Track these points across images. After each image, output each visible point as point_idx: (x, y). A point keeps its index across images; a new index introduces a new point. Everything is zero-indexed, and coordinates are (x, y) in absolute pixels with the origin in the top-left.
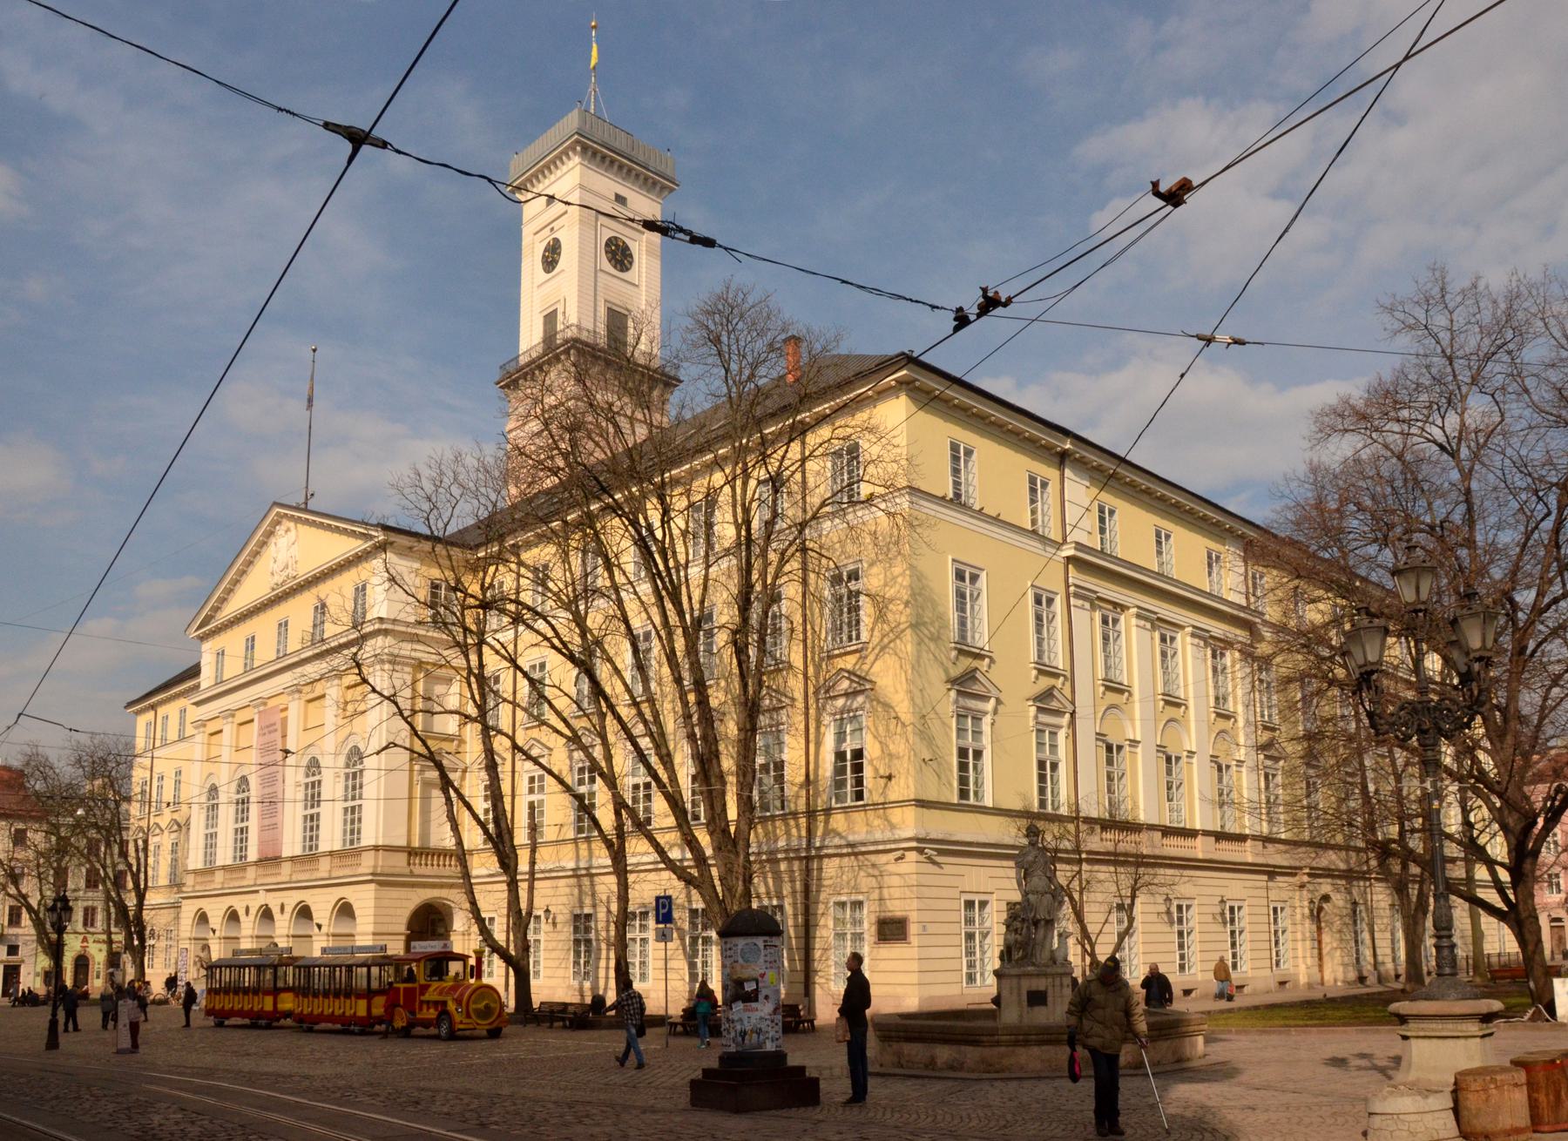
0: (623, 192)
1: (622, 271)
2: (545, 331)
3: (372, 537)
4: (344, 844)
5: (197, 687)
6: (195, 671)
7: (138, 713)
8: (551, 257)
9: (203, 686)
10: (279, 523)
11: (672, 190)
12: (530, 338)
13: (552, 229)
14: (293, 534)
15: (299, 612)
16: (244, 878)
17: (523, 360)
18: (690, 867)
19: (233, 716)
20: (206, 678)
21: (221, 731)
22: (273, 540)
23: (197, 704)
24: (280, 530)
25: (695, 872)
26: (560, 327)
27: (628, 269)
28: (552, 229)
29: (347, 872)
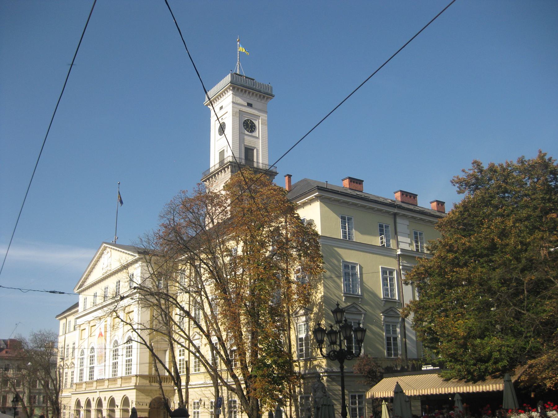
0: (250, 102)
1: (251, 132)
2: (220, 158)
3: (135, 256)
4: (126, 374)
5: (77, 311)
6: (77, 305)
7: (60, 319)
9: (79, 312)
10: (105, 250)
11: (271, 99)
12: (214, 162)
14: (109, 254)
15: (111, 283)
16: (92, 386)
17: (212, 170)
18: (233, 384)
19: (89, 323)
20: (80, 308)
21: (85, 329)
22: (103, 256)
24: (105, 252)
25: (234, 386)
26: (225, 157)
27: (253, 131)
28: (222, 119)
29: (127, 385)
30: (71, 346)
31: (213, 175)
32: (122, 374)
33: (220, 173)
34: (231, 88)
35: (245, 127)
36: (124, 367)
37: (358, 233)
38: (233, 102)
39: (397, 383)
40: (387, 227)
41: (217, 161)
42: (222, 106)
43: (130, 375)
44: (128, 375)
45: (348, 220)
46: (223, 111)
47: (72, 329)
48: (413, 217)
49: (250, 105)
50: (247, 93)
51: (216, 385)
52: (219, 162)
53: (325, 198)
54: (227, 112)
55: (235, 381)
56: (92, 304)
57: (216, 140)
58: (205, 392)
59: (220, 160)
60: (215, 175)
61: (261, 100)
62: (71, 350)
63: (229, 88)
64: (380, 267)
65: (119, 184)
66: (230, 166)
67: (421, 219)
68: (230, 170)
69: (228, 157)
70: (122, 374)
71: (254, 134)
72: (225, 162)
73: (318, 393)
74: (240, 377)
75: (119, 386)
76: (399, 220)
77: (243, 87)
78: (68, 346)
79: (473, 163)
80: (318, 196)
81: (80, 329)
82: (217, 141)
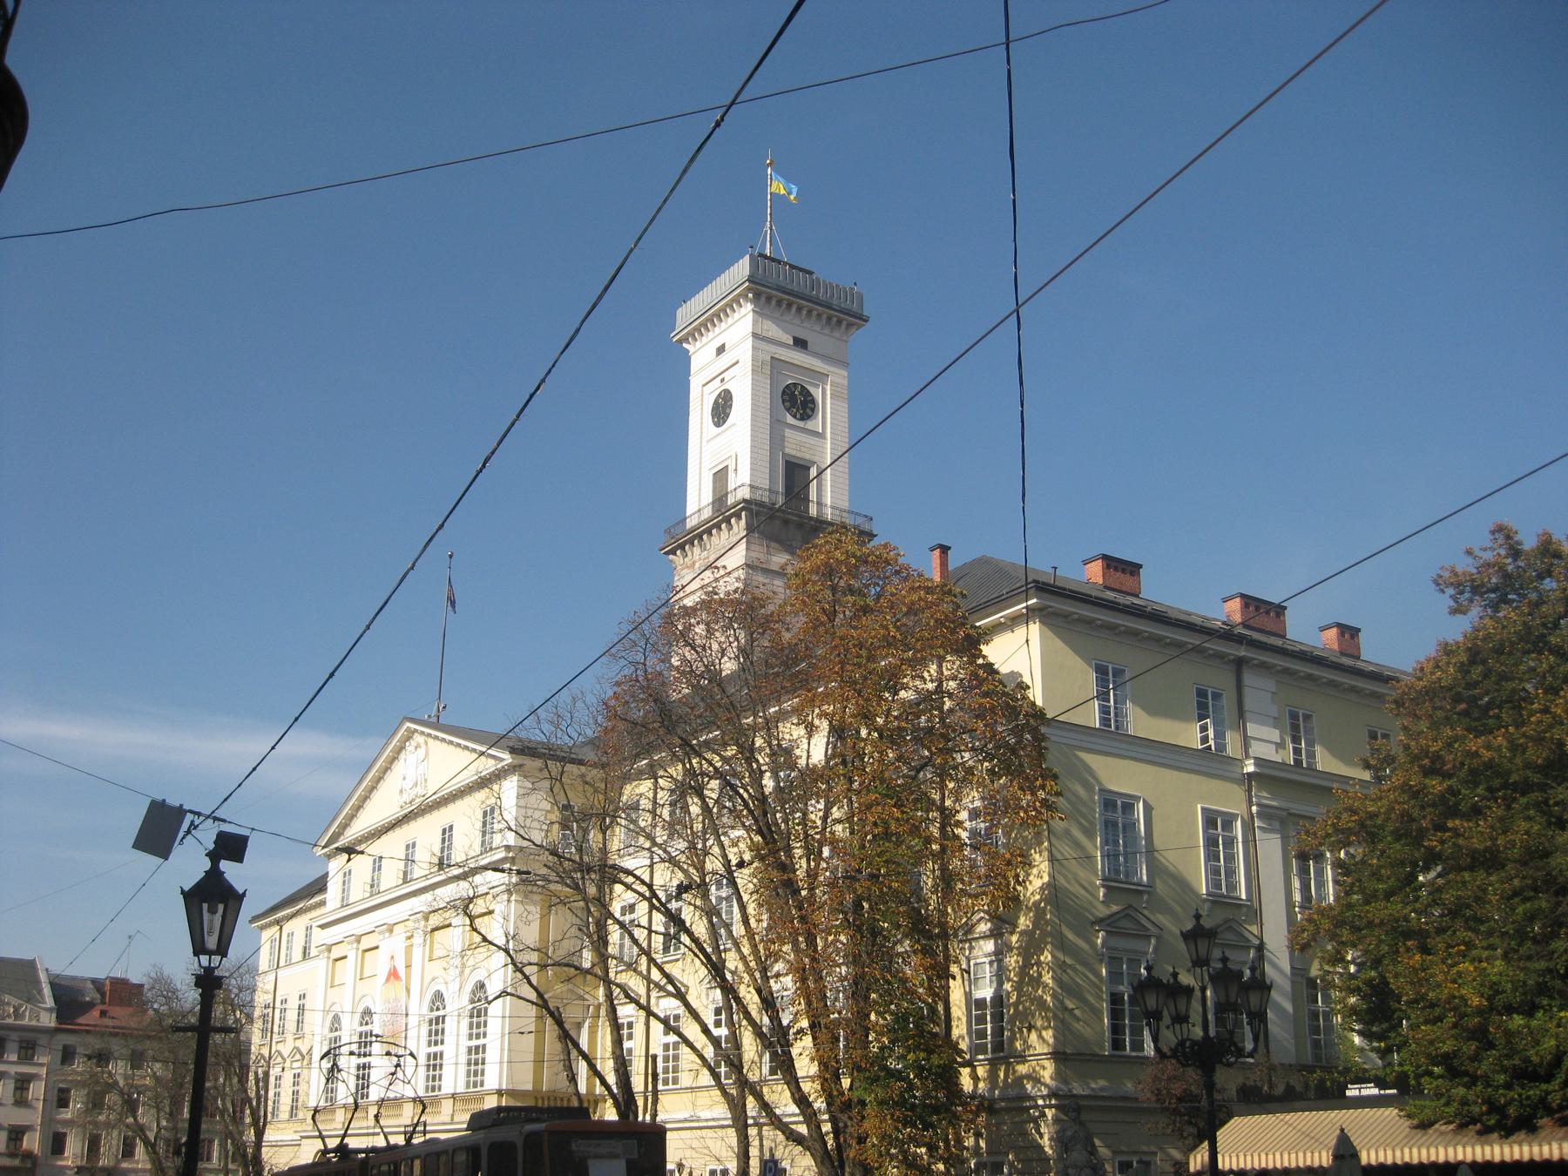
0: (802, 335)
2: (714, 491)
3: (502, 760)
4: (468, 1087)
6: (319, 886)
7: (263, 928)
8: (722, 409)
9: (330, 906)
10: (409, 738)
11: (859, 327)
12: (698, 500)
13: (723, 380)
14: (422, 751)
15: (425, 833)
17: (690, 523)
19: (359, 941)
21: (345, 957)
22: (402, 756)
23: (323, 927)
24: (410, 746)
26: (731, 486)
27: (809, 417)
28: (723, 380)
30: (293, 1004)
31: (695, 537)
32: (455, 1087)
33: (714, 531)
34: (750, 295)
35: (787, 404)
36: (463, 1069)
37: (1139, 710)
38: (755, 335)
39: (1342, 1130)
40: (1216, 696)
41: (708, 498)
42: (723, 346)
43: (479, 1089)
44: (472, 1090)
45: (1114, 676)
46: (726, 359)
47: (297, 954)
48: (1286, 671)
49: (800, 343)
50: (794, 309)
51: (740, 1122)
52: (713, 503)
53: (1054, 614)
54: (737, 362)
55: (803, 1113)
56: (368, 888)
57: (704, 440)
58: (710, 1143)
59: (714, 495)
60: (700, 537)
61: (832, 331)
62: (292, 1016)
63: (744, 295)
64: (1199, 806)
65: (451, 556)
66: (743, 513)
67: (1310, 677)
68: (743, 522)
69: (741, 484)
70: (455, 1087)
71: (810, 425)
72: (731, 500)
73: (1075, 1154)
74: (820, 1104)
75: (448, 1119)
76: (1249, 679)
77: (784, 292)
78: (284, 1001)
79: (1493, 533)
80: (1038, 606)
81: (328, 958)
82: (708, 441)
